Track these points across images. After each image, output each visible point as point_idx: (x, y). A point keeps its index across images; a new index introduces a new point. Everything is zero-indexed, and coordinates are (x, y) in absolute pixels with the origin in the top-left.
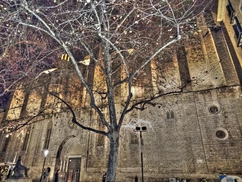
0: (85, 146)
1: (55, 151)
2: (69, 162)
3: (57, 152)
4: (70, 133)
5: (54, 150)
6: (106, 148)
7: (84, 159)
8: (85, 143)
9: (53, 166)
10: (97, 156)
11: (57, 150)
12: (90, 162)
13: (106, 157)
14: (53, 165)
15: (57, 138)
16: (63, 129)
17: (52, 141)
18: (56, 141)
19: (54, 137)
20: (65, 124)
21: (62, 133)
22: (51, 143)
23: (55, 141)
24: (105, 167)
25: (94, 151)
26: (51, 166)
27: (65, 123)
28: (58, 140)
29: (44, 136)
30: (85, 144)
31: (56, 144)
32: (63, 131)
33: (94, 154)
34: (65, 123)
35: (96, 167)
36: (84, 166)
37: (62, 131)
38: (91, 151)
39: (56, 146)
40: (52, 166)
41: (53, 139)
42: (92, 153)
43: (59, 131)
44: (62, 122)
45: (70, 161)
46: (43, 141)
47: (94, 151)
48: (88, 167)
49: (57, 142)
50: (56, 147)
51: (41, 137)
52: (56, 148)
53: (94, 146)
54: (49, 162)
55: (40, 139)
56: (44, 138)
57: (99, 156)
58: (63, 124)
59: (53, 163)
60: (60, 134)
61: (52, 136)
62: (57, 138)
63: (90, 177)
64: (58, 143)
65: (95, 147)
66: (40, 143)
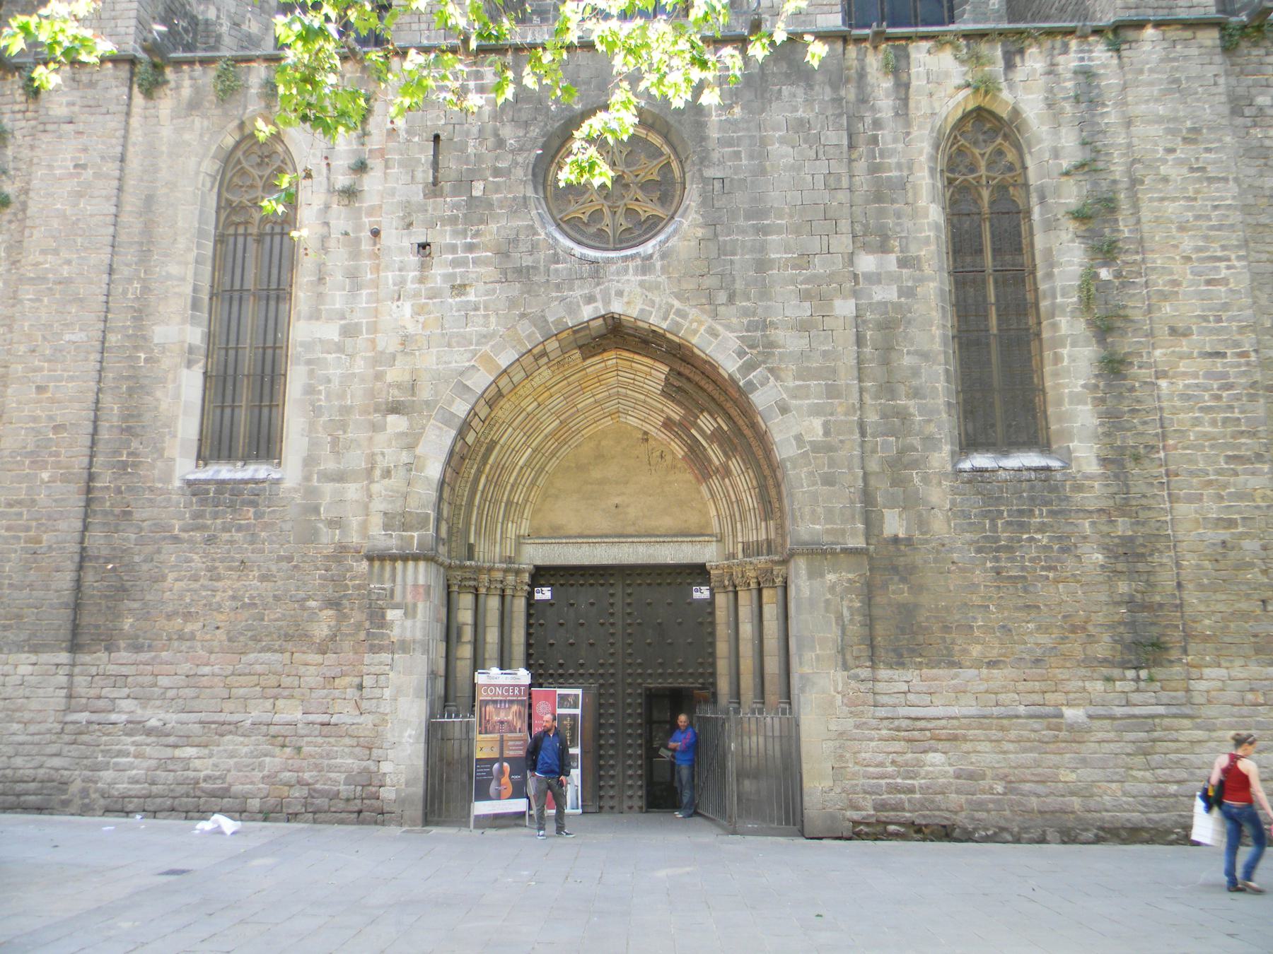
0: (816, 447)
1: (396, 482)
2: (531, 603)
3: (424, 495)
4: (590, 299)
5: (387, 473)
6: (1093, 468)
7: (831, 577)
8: (816, 411)
9: (404, 646)
10: (990, 546)
11: (434, 469)
12: (907, 611)
13: (1099, 557)
14: (395, 634)
15: (406, 340)
16: (470, 248)
17: (334, 372)
18: (394, 374)
19: (349, 331)
20: (497, 186)
21: (460, 289)
22: (310, 390)
23: (379, 376)
24: (1105, 662)
25: (938, 495)
26: (375, 649)
27: (497, 172)
28: (429, 360)
29: (195, 305)
30: (817, 423)
31: (395, 408)
32: (476, 262)
33: (939, 526)
34: (497, 172)
35: (992, 664)
36: (842, 651)
37: (455, 263)
38: (910, 503)
39: (396, 423)
40: (391, 648)
41: (340, 348)
42: (922, 524)
43: (414, 259)
44: (451, 164)
45: (544, 594)
46: (190, 364)
47: (938, 495)
48: (890, 666)
49: (413, 387)
50: (410, 441)
51: (140, 314)
52: (410, 447)
53: (930, 442)
54: (334, 604)
55: (139, 339)
56: (195, 335)
57: (1009, 549)
58: (463, 184)
59: (391, 615)
60: (434, 294)
61: (315, 315)
62: (406, 340)
63: (935, 758)
64: (425, 394)
65: (941, 458)
66: (137, 386)
